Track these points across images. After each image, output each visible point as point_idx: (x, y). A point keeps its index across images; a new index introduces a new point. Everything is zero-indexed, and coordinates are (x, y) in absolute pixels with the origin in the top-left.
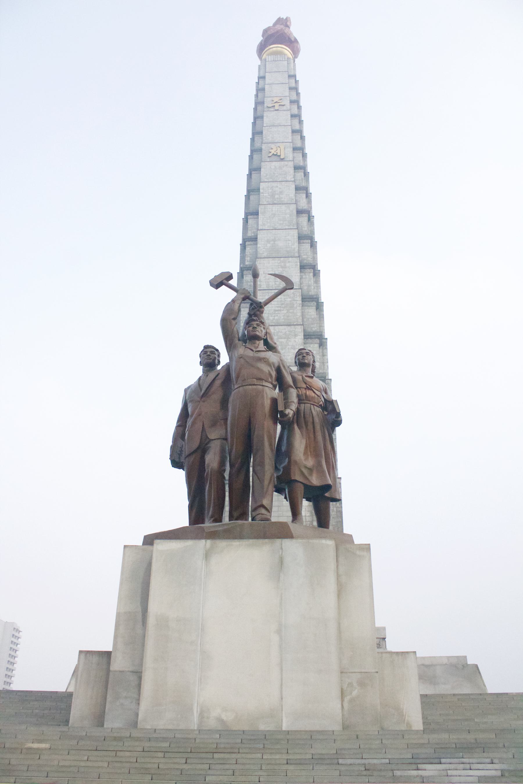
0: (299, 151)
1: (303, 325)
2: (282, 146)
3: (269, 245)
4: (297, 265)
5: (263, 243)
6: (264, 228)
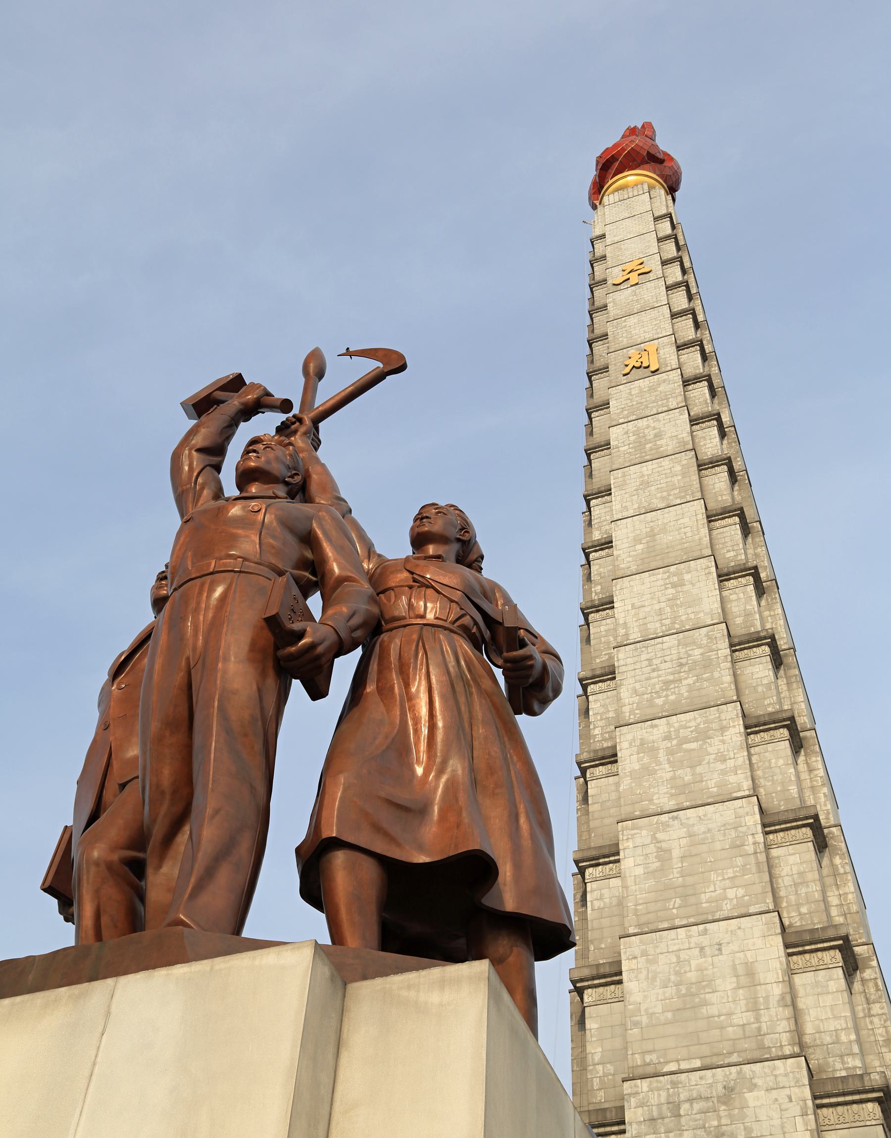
0: (693, 349)
2: (651, 347)
3: (639, 547)
4: (709, 573)
5: (627, 545)
6: (626, 514)
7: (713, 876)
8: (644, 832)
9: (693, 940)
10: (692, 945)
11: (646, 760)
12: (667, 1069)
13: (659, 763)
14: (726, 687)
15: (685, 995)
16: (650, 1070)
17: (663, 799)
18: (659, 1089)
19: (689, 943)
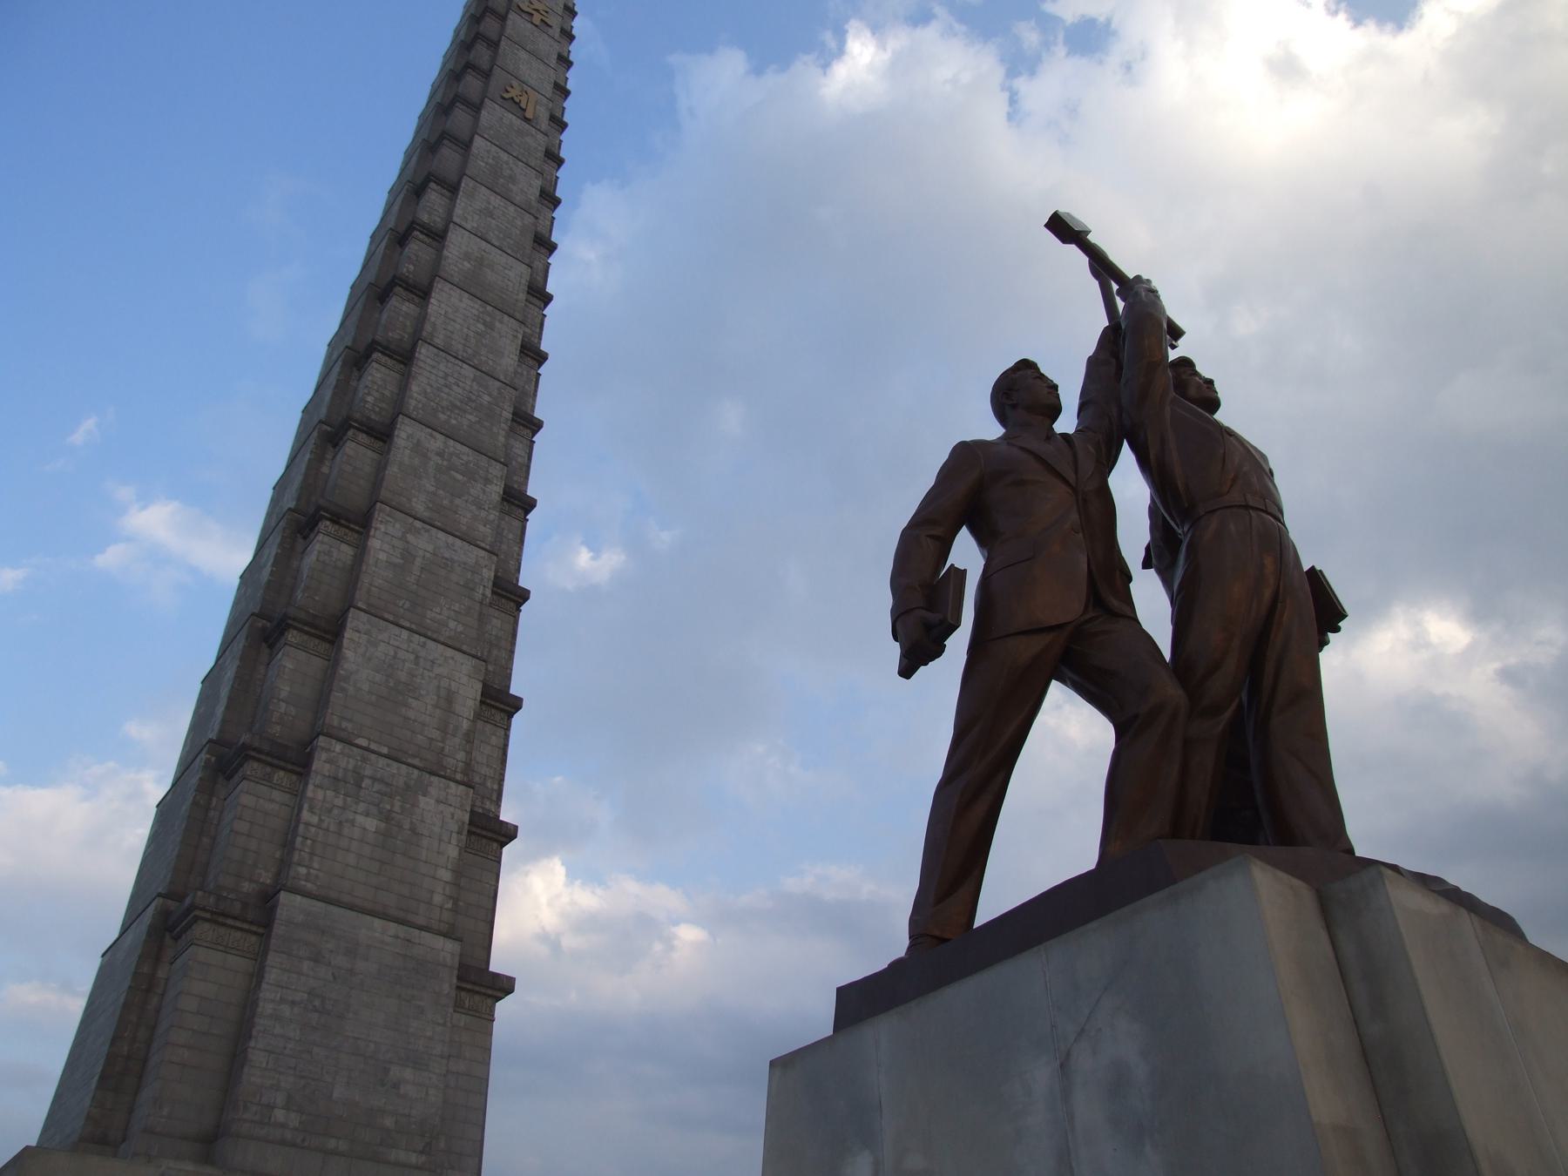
11: (416, 461)
12: (360, 741)
17: (419, 507)
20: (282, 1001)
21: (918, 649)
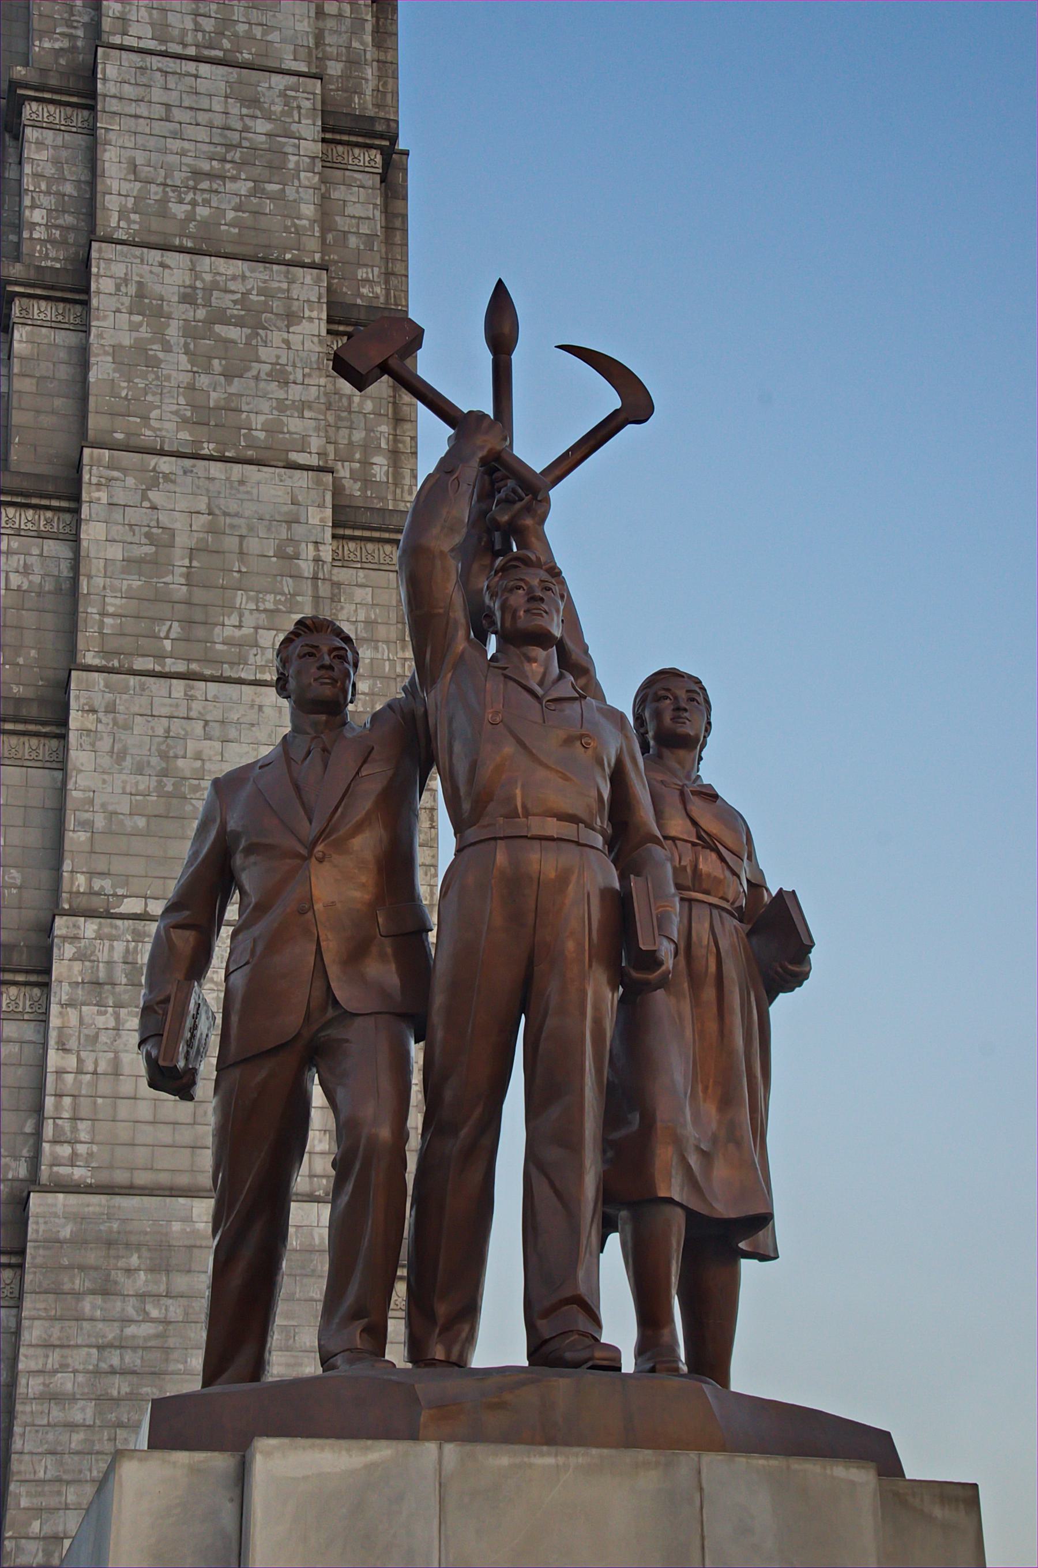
1: (323, 267)
7: (240, 598)
8: (130, 481)
9: (196, 706)
10: (193, 714)
11: (144, 332)
13: (167, 348)
14: (304, 226)
15: (169, 795)
16: (98, 903)
17: (167, 424)
18: (112, 938)
19: (189, 709)
20: (63, 1367)
21: (171, 1079)
